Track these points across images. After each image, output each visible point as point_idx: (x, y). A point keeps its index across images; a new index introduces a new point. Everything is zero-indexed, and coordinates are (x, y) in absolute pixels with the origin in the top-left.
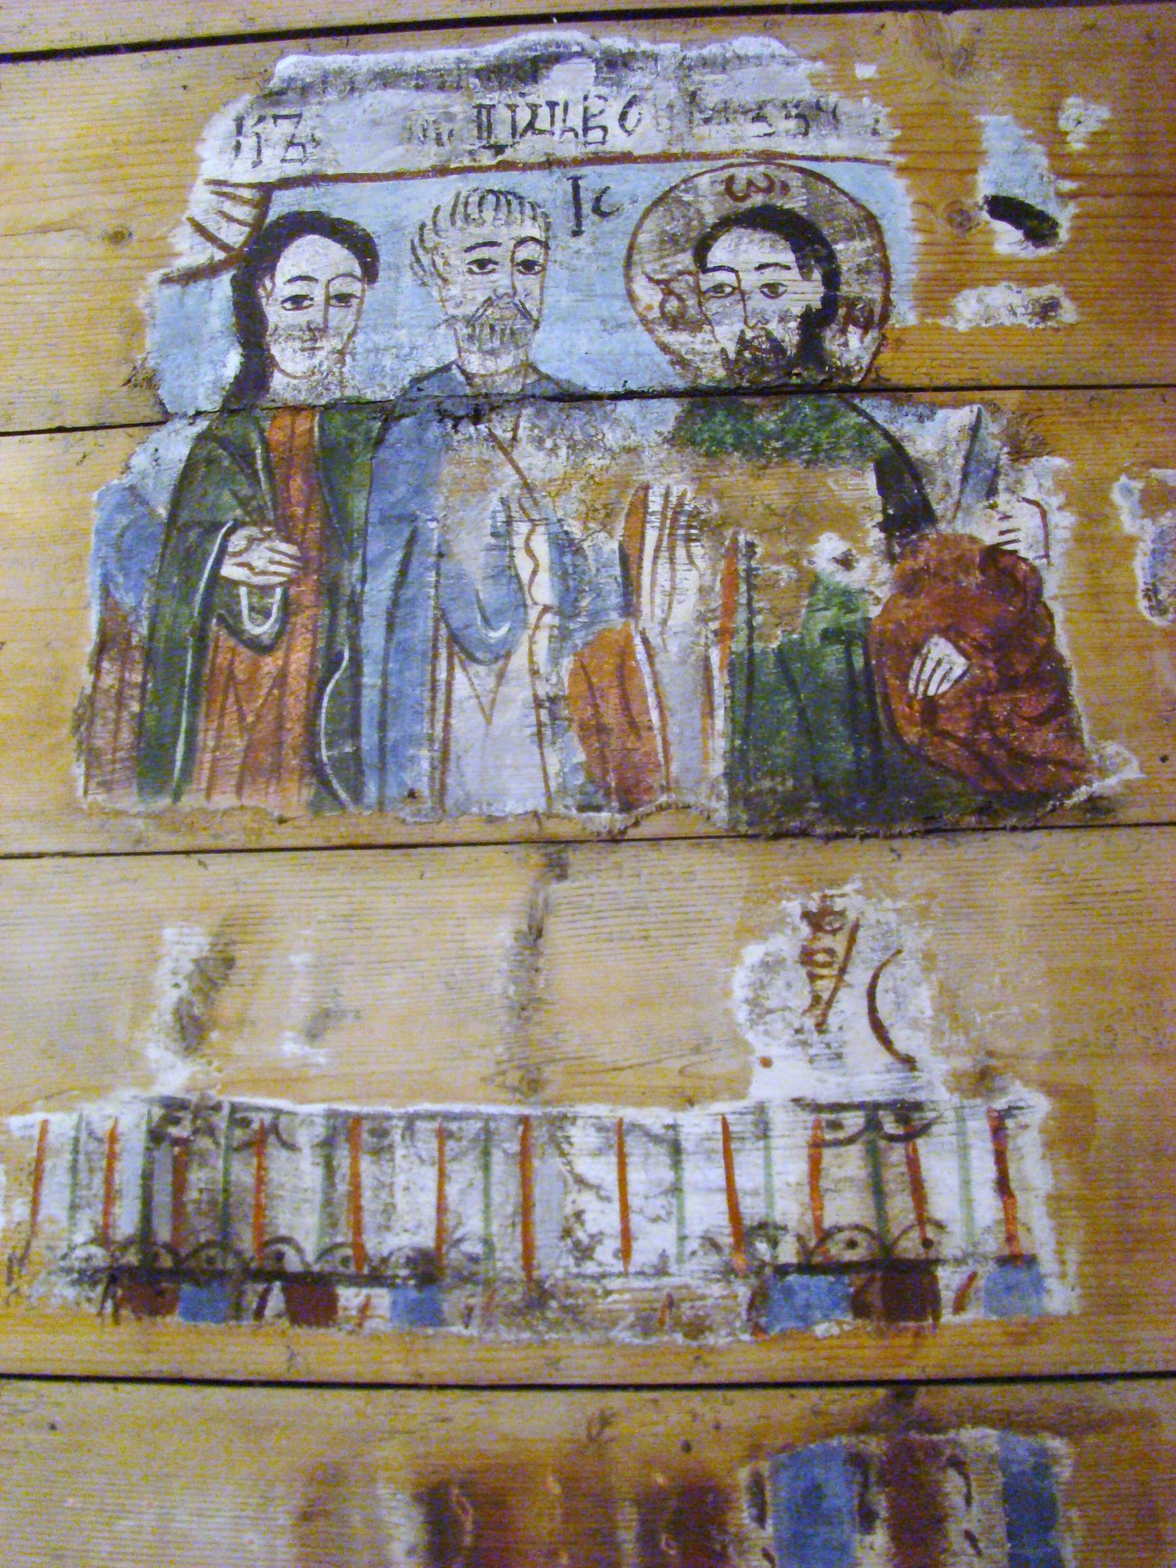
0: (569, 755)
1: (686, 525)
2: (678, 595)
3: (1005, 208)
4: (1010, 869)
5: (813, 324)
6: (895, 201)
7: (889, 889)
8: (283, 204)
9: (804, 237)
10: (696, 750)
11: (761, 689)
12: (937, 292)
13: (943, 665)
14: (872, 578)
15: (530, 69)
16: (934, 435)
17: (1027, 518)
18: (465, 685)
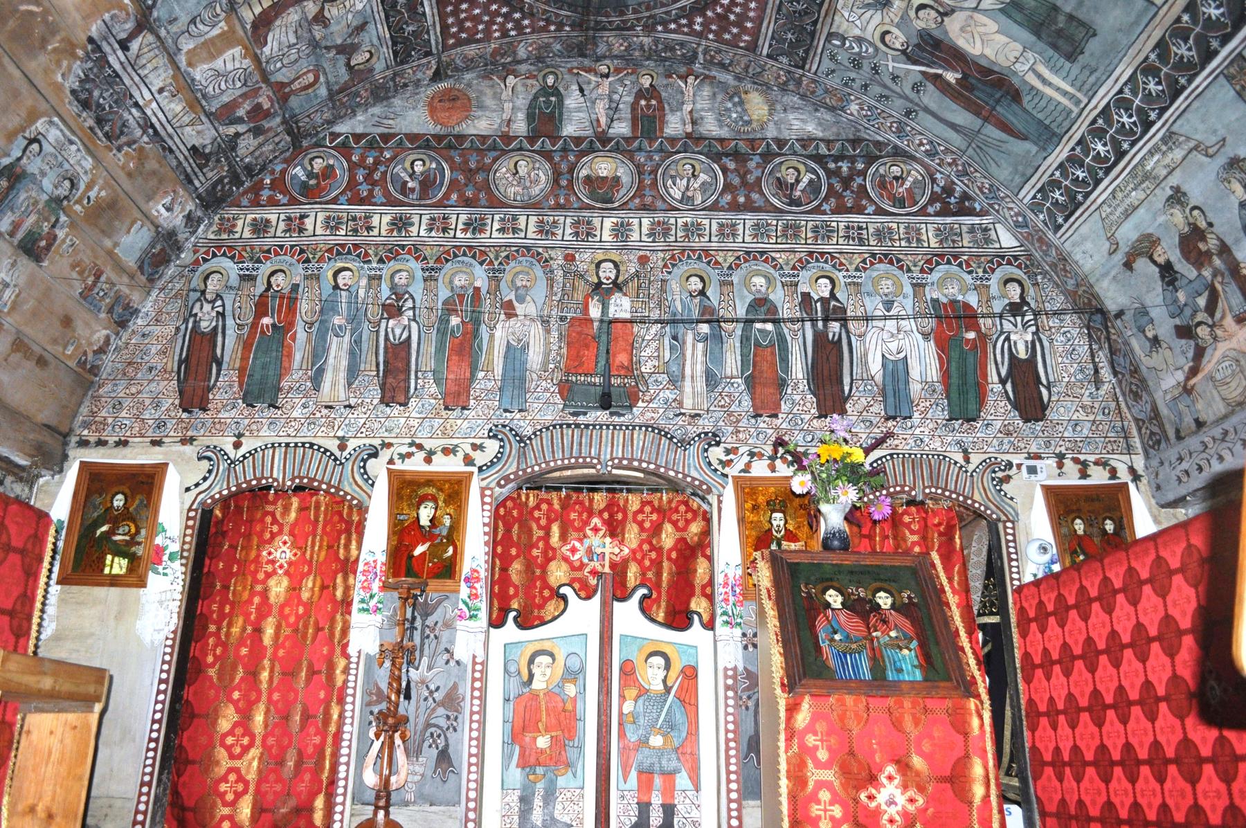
0: (10, 228)
1: (39, 212)
2: (32, 219)
3: (89, 198)
4: (33, 265)
5: (66, 197)
6: (82, 186)
7: (24, 261)
8: (40, 137)
9: (73, 185)
10: (20, 235)
11: (30, 233)
12: (77, 202)
13: (43, 243)
14: (46, 230)
15: (71, 142)
16: (63, 218)
17: (61, 234)
18: (9, 213)
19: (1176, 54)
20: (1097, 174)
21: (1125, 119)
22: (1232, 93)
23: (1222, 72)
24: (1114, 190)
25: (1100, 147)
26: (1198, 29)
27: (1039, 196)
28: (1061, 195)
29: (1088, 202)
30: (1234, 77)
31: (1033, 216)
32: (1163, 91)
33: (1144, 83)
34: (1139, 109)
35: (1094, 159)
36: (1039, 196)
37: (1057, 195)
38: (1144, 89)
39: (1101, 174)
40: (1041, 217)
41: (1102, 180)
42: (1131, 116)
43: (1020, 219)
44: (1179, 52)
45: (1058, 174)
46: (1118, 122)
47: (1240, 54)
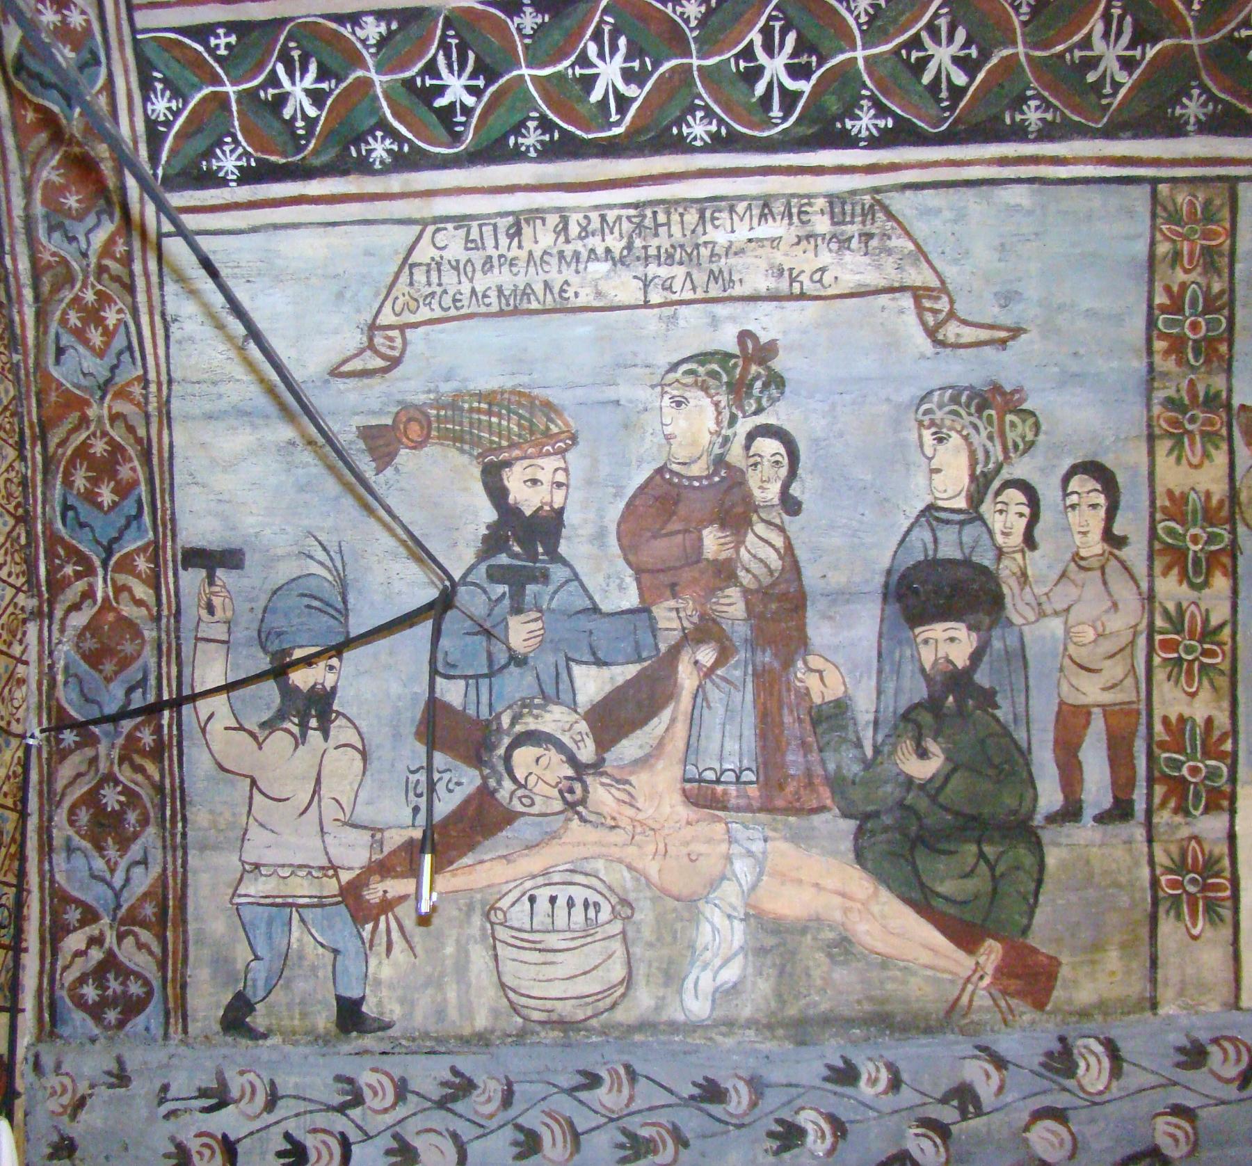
19: (1086, 43)
20: (518, 129)
21: (775, 67)
22: (1140, 248)
23: (1154, 182)
24: (536, 215)
25: (609, 72)
26: (1194, 42)
27: (222, 41)
28: (317, 97)
29: (395, 183)
30: (1174, 217)
31: (125, 82)
32: (957, 93)
33: (932, 29)
34: (846, 73)
35: (552, 88)
36: (222, 41)
37: (297, 92)
38: (916, 43)
39: (532, 138)
40: (161, 106)
41: (517, 155)
42: (797, 72)
43: (66, 55)
44: (1099, 46)
45: (373, 30)
46: (748, 53)
47: (1233, 181)
